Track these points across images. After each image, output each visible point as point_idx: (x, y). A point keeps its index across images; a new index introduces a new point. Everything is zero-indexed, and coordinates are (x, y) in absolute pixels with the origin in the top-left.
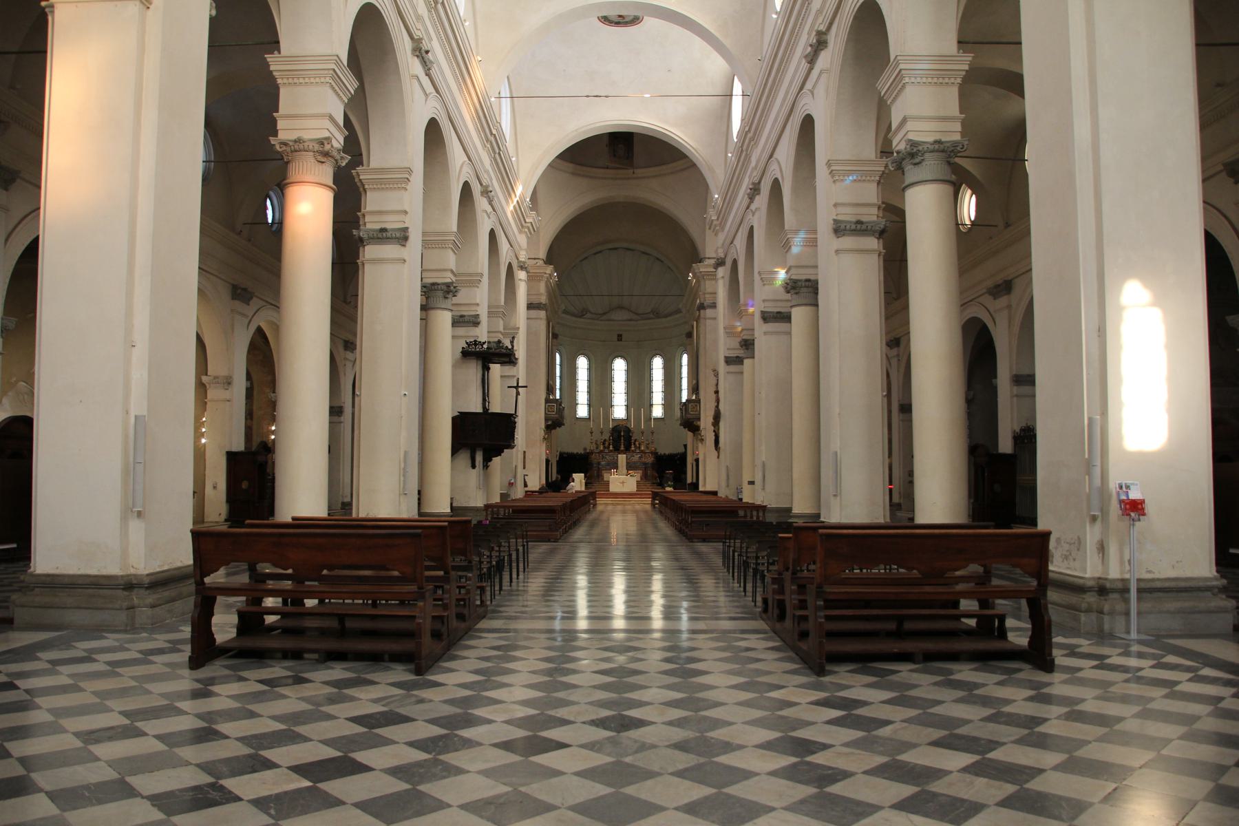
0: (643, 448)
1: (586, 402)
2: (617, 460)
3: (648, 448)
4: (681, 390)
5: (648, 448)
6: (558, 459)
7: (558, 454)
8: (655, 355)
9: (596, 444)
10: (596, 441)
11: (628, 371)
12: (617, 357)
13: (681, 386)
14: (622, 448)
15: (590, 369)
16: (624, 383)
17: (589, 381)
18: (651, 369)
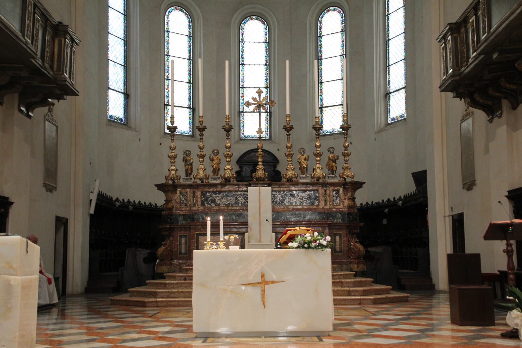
0: (318, 172)
1: (186, 103)
2: (245, 206)
3: (333, 171)
4: (387, 67)
5: (333, 171)
6: (92, 211)
7: (94, 197)
8: (325, 9)
9: (185, 160)
10: (187, 153)
11: (269, 43)
12: (251, 15)
13: (386, 57)
14: (260, 173)
15: (192, 37)
16: (263, 68)
17: (192, 61)
18: (318, 37)
